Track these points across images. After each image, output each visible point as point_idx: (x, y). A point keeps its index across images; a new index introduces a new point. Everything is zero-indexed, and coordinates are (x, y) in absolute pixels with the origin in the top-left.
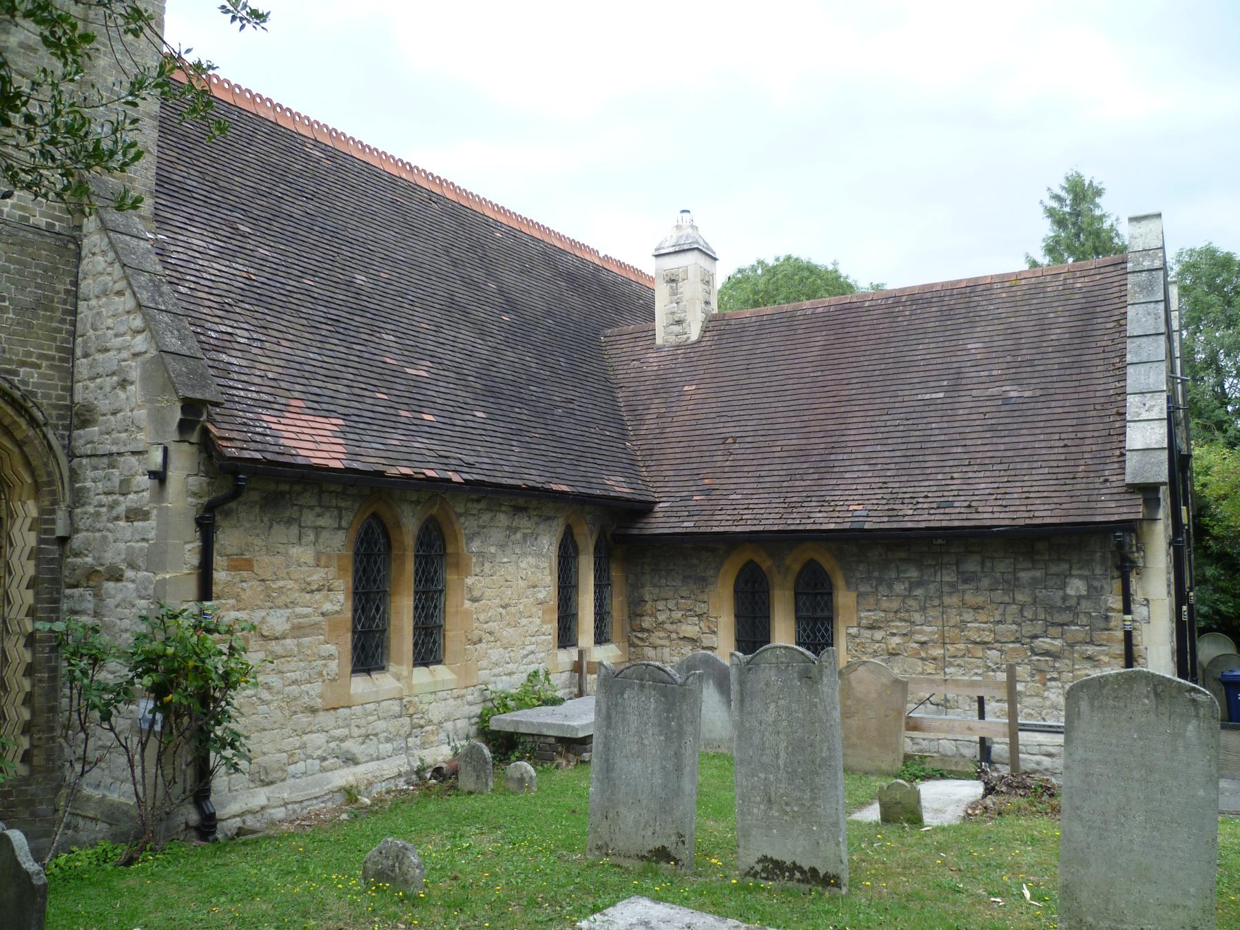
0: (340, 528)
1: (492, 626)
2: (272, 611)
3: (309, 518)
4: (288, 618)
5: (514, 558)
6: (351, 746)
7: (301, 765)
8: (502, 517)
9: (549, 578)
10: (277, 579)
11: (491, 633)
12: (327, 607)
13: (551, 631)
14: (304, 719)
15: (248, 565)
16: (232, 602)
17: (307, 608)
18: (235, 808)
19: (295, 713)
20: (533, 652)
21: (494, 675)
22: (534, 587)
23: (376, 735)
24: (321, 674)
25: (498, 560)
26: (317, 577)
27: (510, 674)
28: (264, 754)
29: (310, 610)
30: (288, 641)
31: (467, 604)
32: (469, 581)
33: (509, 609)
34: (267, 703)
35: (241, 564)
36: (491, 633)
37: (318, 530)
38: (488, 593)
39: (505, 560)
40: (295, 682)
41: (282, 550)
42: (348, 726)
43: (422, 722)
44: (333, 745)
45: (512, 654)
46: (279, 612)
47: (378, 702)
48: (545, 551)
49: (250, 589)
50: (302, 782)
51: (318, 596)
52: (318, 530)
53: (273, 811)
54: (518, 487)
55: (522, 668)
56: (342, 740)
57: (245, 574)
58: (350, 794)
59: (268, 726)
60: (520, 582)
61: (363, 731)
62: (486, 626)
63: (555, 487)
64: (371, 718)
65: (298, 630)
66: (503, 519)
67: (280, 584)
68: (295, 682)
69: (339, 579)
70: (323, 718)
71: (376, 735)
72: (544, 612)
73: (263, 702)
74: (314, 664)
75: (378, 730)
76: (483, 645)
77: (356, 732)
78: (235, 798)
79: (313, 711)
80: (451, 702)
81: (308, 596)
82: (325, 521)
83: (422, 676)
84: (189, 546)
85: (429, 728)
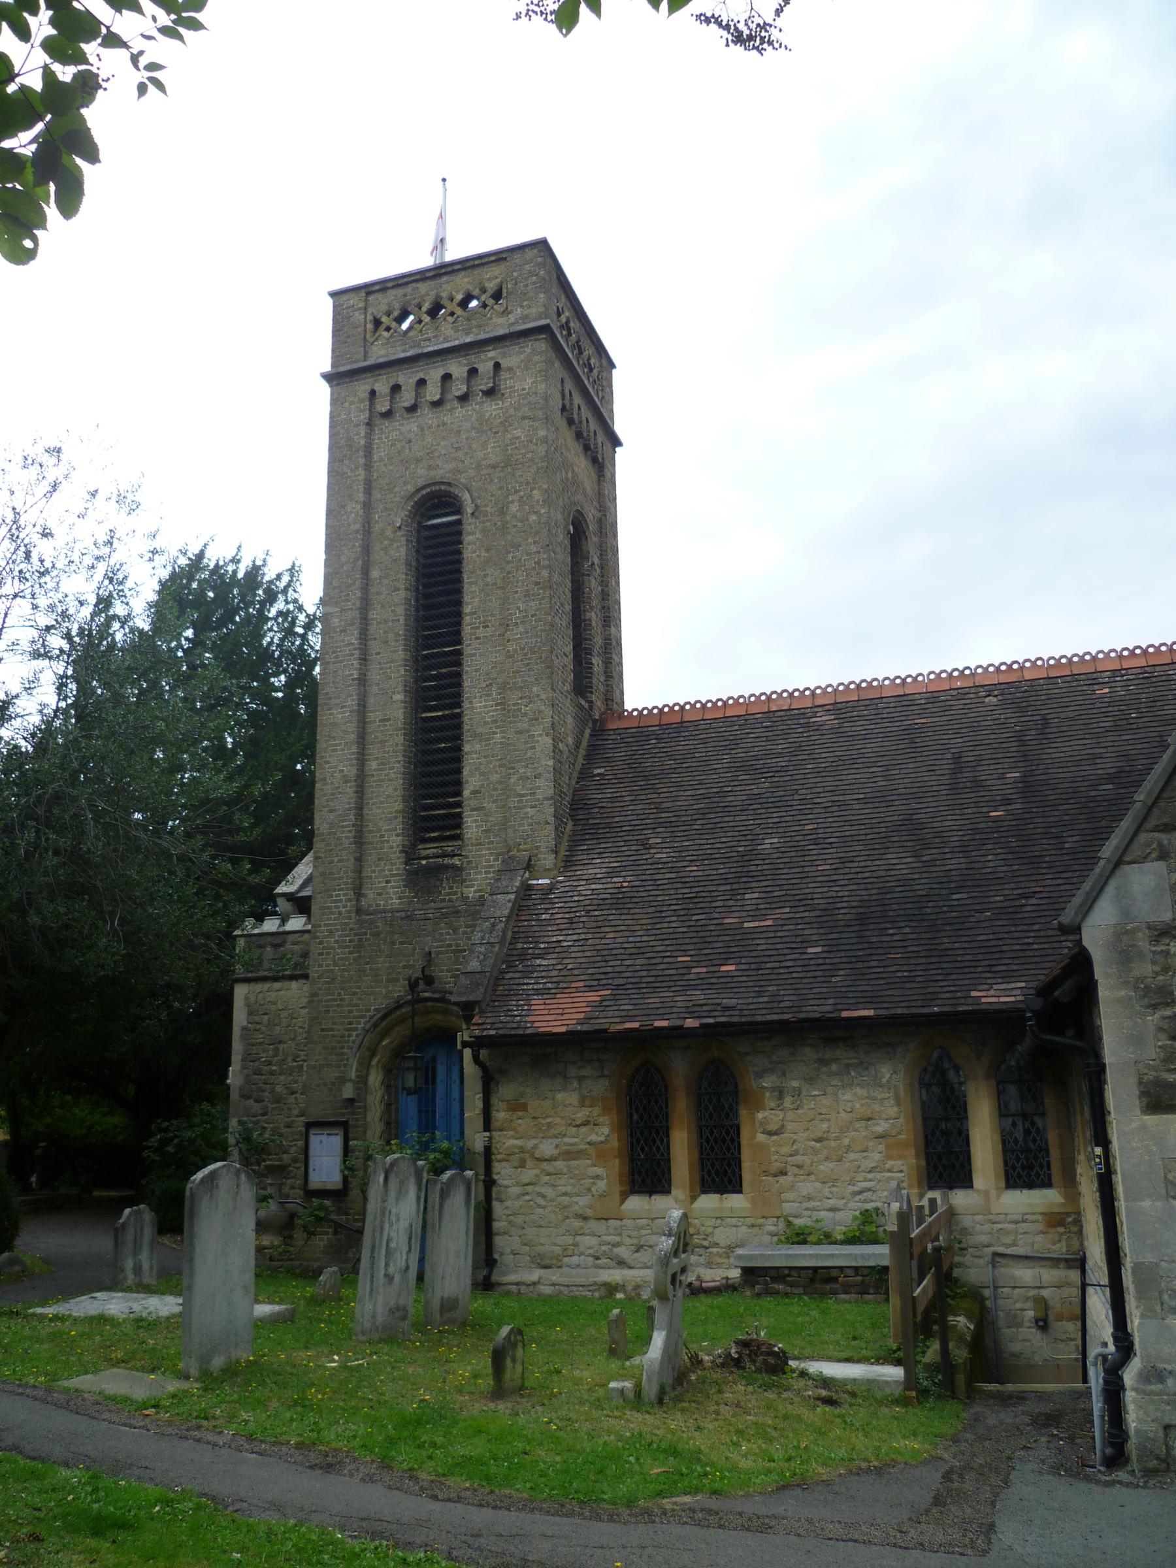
0: (603, 1076)
1: (798, 1159)
2: (544, 1141)
3: (572, 1071)
4: (557, 1146)
5: (830, 1090)
6: (623, 1252)
7: (575, 1260)
8: (807, 1050)
9: (895, 1109)
10: (547, 1117)
11: (798, 1166)
12: (593, 1138)
13: (904, 1168)
14: (577, 1224)
15: (524, 1107)
16: (511, 1133)
17: (575, 1139)
18: (512, 1278)
19: (567, 1217)
20: (869, 1190)
21: (807, 1209)
22: (869, 1119)
23: (651, 1247)
24: (589, 1190)
25: (804, 1093)
26: (582, 1115)
27: (833, 1210)
28: (542, 1244)
29: (576, 1140)
30: (559, 1163)
31: (761, 1137)
32: (760, 1116)
33: (825, 1143)
34: (544, 1207)
35: (517, 1106)
36: (798, 1166)
37: (581, 1079)
38: (790, 1126)
39: (817, 1093)
40: (565, 1194)
41: (549, 1095)
42: (620, 1234)
43: (706, 1243)
44: (604, 1248)
45: (834, 1189)
46: (550, 1141)
47: (653, 1219)
48: (884, 1080)
49: (524, 1124)
50: (574, 1272)
51: (583, 1129)
52: (581, 1079)
53: (542, 1287)
54: (786, 1022)
55: (852, 1205)
56: (613, 1245)
57: (520, 1114)
58: (611, 1289)
59: (543, 1224)
60: (843, 1115)
61: (635, 1241)
62: (790, 1159)
63: (844, 1014)
64: (644, 1232)
65: (569, 1155)
66: (809, 1053)
67: (549, 1120)
68: (565, 1194)
69: (604, 1115)
70: (592, 1225)
71: (651, 1247)
72: (889, 1147)
73: (539, 1206)
74: (582, 1182)
75: (651, 1243)
76: (789, 1178)
77: (628, 1241)
78: (516, 1272)
79: (585, 1219)
80: (744, 1229)
81: (574, 1129)
82: (587, 1071)
83: (708, 1202)
84: (477, 1096)
85: (714, 1250)
